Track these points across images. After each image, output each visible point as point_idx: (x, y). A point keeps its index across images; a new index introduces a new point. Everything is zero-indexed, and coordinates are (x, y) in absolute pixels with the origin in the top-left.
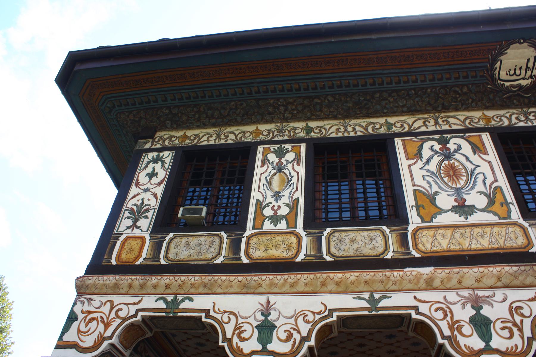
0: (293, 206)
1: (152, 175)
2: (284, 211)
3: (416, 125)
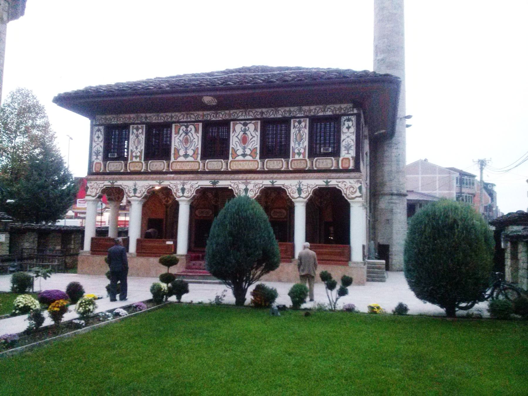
0: (141, 152)
1: (98, 137)
2: (138, 154)
3: (180, 118)
